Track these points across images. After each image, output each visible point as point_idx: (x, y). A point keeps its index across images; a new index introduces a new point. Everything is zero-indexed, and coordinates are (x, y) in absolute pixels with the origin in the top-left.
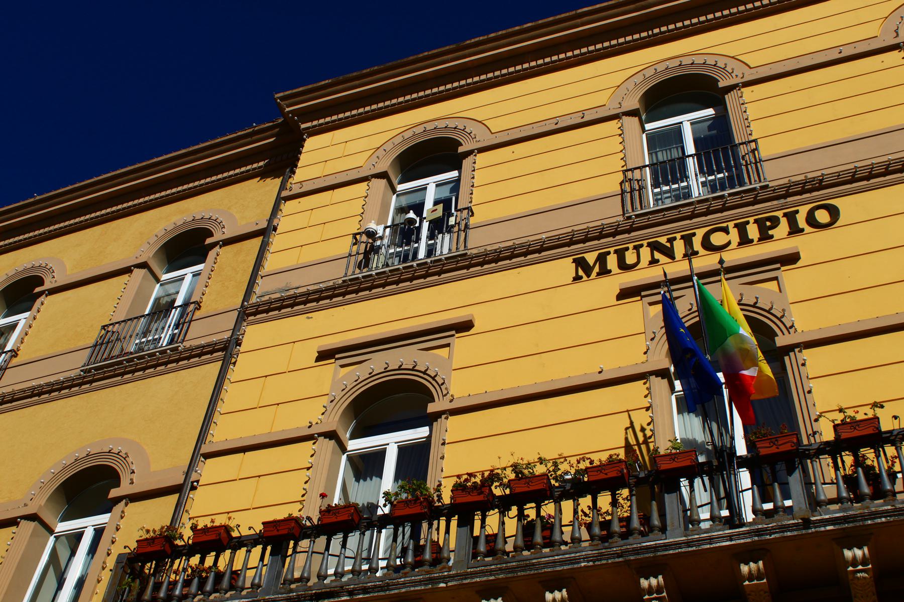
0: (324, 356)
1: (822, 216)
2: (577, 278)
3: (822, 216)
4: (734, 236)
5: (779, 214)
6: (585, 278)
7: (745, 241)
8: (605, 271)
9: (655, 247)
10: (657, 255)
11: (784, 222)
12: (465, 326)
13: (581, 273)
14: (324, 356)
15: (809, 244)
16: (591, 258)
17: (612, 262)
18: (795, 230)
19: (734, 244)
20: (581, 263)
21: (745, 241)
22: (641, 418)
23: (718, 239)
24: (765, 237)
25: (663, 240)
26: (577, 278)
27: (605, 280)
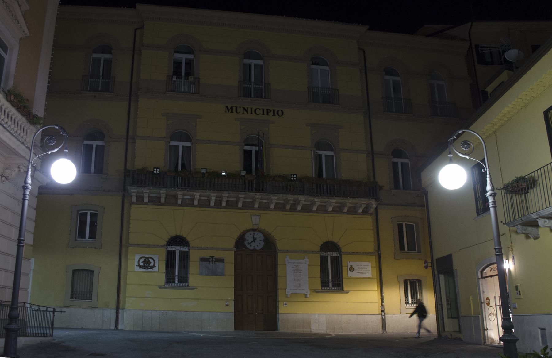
1: (280, 113)
3: (280, 113)
5: (271, 109)
9: (244, 108)
10: (245, 112)
11: (272, 111)
17: (234, 109)
20: (227, 107)
21: (263, 114)
25: (246, 107)
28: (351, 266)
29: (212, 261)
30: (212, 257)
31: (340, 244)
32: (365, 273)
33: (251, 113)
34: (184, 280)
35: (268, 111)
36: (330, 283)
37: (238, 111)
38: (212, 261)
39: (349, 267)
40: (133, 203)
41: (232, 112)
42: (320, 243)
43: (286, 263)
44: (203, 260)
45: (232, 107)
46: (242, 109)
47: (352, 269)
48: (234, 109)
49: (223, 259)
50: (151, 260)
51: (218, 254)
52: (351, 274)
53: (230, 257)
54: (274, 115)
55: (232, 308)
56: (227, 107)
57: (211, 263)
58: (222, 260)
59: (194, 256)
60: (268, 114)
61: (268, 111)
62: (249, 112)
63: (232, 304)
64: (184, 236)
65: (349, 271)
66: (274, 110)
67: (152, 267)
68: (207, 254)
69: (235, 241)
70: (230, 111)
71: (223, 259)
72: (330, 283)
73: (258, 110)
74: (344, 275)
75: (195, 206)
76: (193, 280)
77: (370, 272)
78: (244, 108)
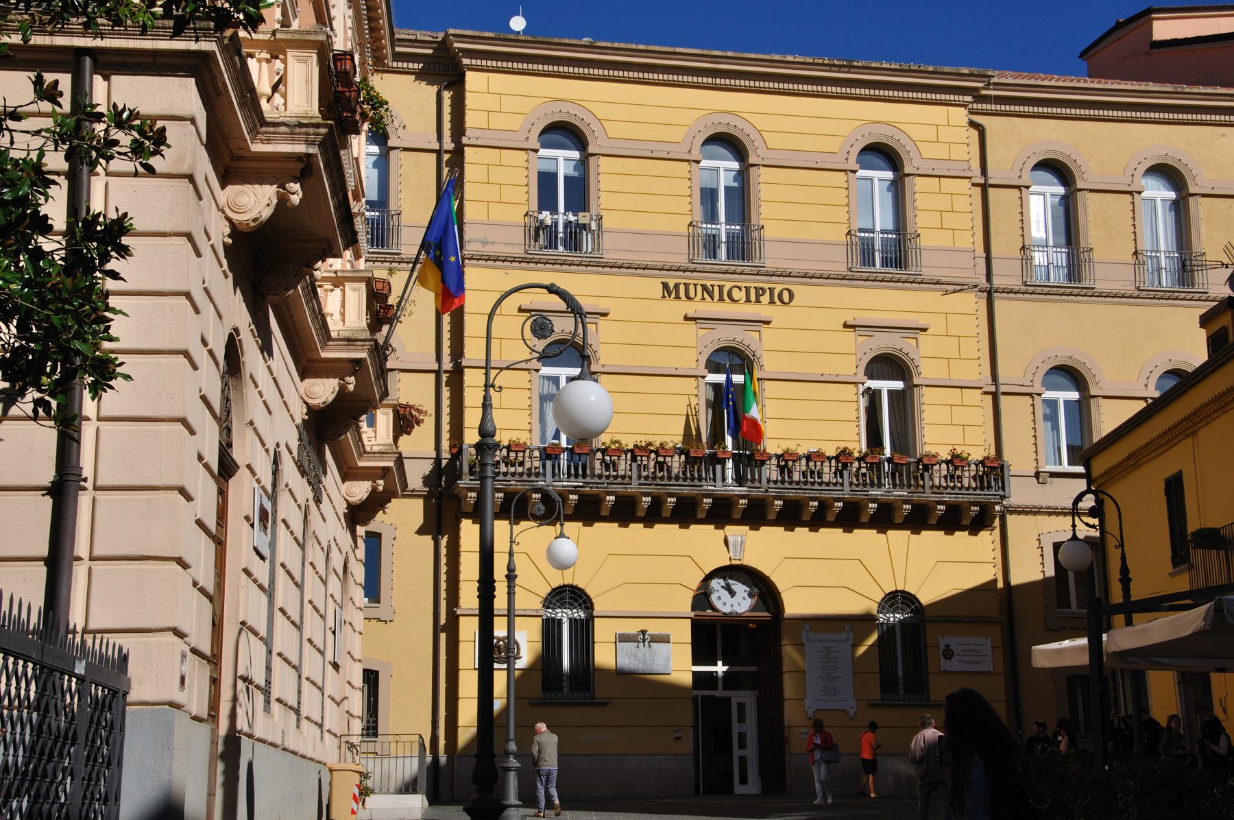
2: (664, 297)
4: (743, 294)
5: (766, 286)
7: (748, 300)
8: (678, 297)
9: (704, 288)
10: (706, 295)
15: (774, 312)
16: (671, 283)
17: (682, 288)
20: (665, 286)
21: (748, 300)
22: (694, 401)
23: (737, 294)
24: (758, 301)
25: (708, 283)
28: (947, 646)
30: (643, 632)
32: (979, 663)
33: (721, 299)
35: (760, 292)
36: (901, 686)
37: (692, 294)
39: (942, 648)
41: (678, 297)
43: (804, 641)
44: (624, 638)
45: (677, 286)
46: (699, 289)
47: (948, 654)
48: (682, 288)
49: (668, 636)
51: (654, 628)
52: (945, 665)
53: (682, 632)
54: (772, 302)
56: (665, 286)
58: (665, 639)
60: (758, 301)
61: (760, 292)
62: (716, 296)
63: (689, 735)
64: (581, 586)
65: (942, 658)
68: (632, 627)
69: (692, 594)
70: (673, 295)
71: (668, 636)
72: (901, 686)
73: (735, 291)
78: (704, 288)
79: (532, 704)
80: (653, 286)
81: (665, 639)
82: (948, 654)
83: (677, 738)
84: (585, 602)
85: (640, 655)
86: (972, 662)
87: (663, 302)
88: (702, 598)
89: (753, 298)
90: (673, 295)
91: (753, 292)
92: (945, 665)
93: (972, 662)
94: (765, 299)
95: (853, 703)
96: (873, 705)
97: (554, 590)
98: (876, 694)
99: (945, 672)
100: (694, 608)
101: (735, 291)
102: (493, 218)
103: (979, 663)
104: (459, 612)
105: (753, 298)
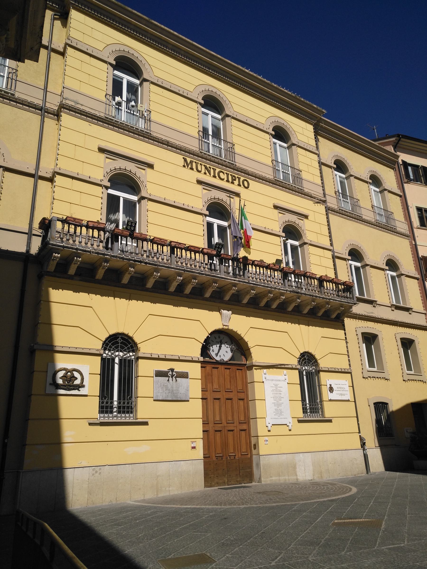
0: (101, 150)
1: (246, 183)
2: (184, 166)
5: (236, 176)
6: (186, 167)
7: (228, 181)
8: (192, 169)
9: (206, 168)
12: (151, 166)
13: (186, 165)
14: (101, 150)
16: (189, 160)
18: (239, 185)
19: (225, 180)
20: (185, 160)
24: (232, 183)
25: (208, 166)
26: (184, 166)
27: (191, 171)
28: (330, 385)
29: (172, 376)
30: (172, 370)
31: (137, 339)
32: (344, 395)
34: (127, 406)
38: (172, 376)
39: (329, 386)
40: (49, 274)
42: (104, 336)
43: (264, 380)
44: (159, 374)
45: (191, 162)
48: (194, 164)
49: (187, 373)
50: (76, 374)
51: (179, 367)
54: (239, 185)
55: (200, 453)
57: (170, 378)
58: (184, 375)
59: (145, 369)
63: (200, 444)
66: (239, 179)
67: (78, 387)
68: (164, 366)
71: (187, 373)
74: (325, 398)
75: (147, 290)
76: (144, 408)
77: (348, 393)
79: (90, 424)
80: (178, 159)
81: (184, 375)
82: (331, 389)
83: (194, 448)
84: (132, 347)
85: (169, 387)
86: (341, 395)
87: (184, 168)
88: (205, 350)
89: (230, 180)
90: (190, 166)
91: (230, 177)
92: (332, 396)
93: (341, 395)
94: (236, 182)
95: (291, 420)
96: (300, 421)
97: (110, 336)
98: (300, 414)
99: (330, 400)
100: (202, 355)
101: (221, 174)
102: (83, 91)
103: (344, 395)
104: (36, 347)
105: (230, 180)
